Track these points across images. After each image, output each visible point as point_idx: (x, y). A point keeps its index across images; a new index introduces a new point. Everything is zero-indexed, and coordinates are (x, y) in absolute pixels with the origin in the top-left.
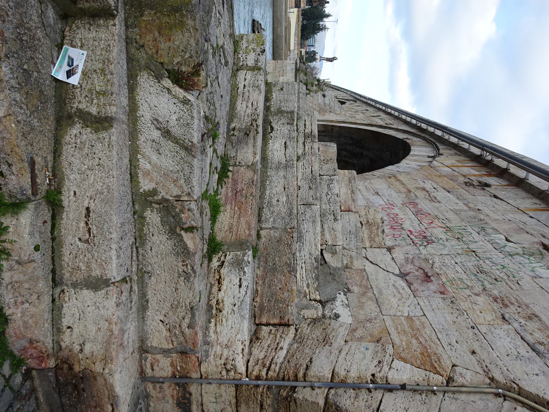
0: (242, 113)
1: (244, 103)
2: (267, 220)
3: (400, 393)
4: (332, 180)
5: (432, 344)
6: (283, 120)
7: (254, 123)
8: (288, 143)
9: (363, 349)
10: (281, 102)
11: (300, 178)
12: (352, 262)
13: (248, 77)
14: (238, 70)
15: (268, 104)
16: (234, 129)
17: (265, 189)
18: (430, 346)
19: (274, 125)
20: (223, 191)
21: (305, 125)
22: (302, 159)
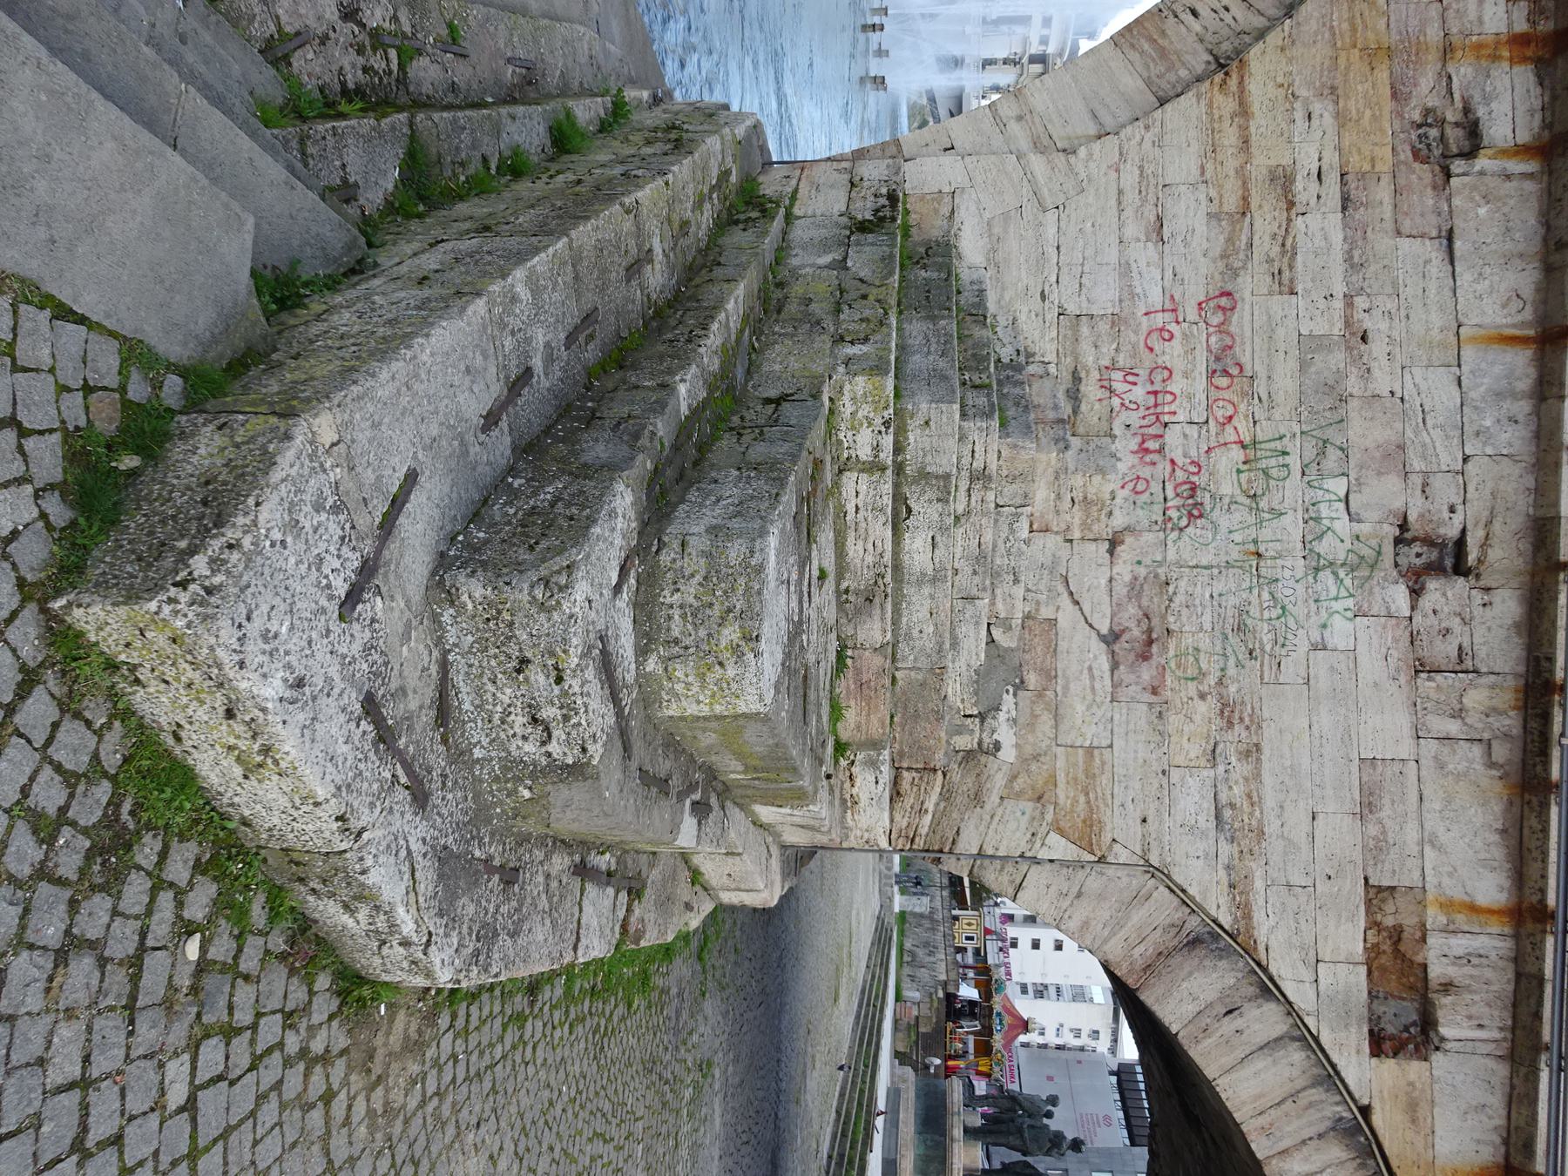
0: (857, 561)
1: (860, 543)
2: (904, 659)
3: (1048, 866)
4: (1018, 515)
6: (931, 494)
7: (880, 582)
8: (938, 538)
9: (1019, 814)
11: (957, 556)
13: (863, 488)
14: (841, 471)
16: (847, 591)
17: (900, 616)
20: (843, 683)
22: (963, 521)
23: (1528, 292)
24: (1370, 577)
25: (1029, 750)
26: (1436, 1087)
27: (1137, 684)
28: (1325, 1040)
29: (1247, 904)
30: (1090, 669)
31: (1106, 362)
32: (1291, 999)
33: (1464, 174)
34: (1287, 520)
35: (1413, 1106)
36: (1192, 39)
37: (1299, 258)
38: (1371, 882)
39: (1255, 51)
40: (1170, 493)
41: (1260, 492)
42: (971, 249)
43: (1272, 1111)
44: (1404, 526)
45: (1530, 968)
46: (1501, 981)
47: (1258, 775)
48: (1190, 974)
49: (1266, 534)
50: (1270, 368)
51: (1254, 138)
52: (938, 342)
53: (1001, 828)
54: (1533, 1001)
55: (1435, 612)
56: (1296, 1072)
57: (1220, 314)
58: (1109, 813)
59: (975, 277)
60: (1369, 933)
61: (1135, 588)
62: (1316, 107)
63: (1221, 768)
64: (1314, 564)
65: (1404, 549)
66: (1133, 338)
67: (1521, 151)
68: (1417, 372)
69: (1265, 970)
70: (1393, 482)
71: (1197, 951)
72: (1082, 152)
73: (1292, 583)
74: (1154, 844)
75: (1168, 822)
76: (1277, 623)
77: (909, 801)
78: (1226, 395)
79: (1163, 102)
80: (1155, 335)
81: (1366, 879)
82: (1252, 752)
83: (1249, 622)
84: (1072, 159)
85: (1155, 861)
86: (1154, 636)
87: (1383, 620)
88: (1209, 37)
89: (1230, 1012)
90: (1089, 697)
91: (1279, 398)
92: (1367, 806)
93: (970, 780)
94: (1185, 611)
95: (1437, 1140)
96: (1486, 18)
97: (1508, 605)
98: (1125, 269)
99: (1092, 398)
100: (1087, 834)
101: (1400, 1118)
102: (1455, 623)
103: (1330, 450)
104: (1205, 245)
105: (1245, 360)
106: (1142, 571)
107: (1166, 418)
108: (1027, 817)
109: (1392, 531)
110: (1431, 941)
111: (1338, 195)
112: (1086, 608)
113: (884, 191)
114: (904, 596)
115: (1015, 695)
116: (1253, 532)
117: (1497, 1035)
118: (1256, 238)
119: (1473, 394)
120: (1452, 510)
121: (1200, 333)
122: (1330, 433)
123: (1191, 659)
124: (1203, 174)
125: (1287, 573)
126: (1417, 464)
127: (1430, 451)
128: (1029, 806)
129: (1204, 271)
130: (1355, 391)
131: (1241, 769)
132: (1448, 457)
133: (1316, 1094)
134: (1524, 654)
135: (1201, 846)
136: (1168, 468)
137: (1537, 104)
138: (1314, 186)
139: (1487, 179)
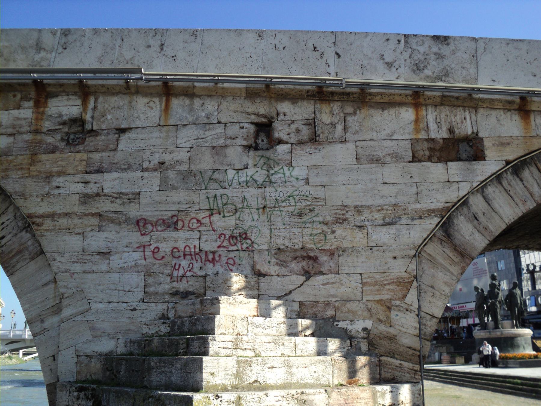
3: (421, 302)
5: (390, 277)
7: (296, 397)
8: (269, 365)
9: (398, 318)
10: (228, 374)
12: (295, 311)
15: (230, 388)
17: (307, 383)
18: (391, 279)
19: (252, 380)
21: (223, 348)
22: (257, 352)
23: (146, 100)
24: (274, 160)
25: (366, 314)
26: (493, 135)
27: (329, 262)
28: (482, 179)
29: (428, 211)
30: (323, 284)
31: (168, 279)
32: (467, 192)
33: (92, 124)
34: (247, 195)
35: (503, 144)
36: (14, 239)
37: (123, 191)
38: (411, 160)
39: (25, 211)
40: (234, 248)
41: (234, 207)
42: (106, 346)
43: (515, 200)
44: (248, 147)
45: (439, 100)
46: (445, 111)
47: (369, 207)
48: (462, 235)
49: (254, 204)
50: (174, 203)
51: (65, 211)
52: (165, 367)
53: (405, 326)
54: (452, 99)
55: (289, 134)
56: (497, 190)
57: (147, 226)
58: (393, 274)
59: (122, 345)
60: (433, 161)
61: (282, 264)
62: (55, 184)
63: (367, 223)
64: (268, 183)
65: (260, 146)
66: (157, 266)
67: (85, 103)
68: (179, 141)
69: (456, 204)
70: (230, 151)
71: (452, 233)
72: (62, 290)
73: (277, 193)
74: (405, 253)
75: (394, 246)
76: (297, 199)
77: (397, 374)
78: (186, 222)
79: (42, 252)
80: (156, 255)
81: (410, 162)
82: (358, 209)
83: (296, 212)
84: (66, 295)
85: (413, 252)
86: (305, 254)
87: (293, 155)
88: (14, 232)
89: (476, 218)
90: (337, 284)
91: (188, 199)
92: (377, 161)
93: (383, 342)
94: (292, 241)
95: (514, 135)
96: (25, 116)
97: (285, 107)
98: (122, 270)
99: (186, 285)
100: (405, 285)
101: (508, 149)
102: (293, 127)
103: (213, 177)
104: (114, 232)
105: (170, 214)
106: (273, 261)
107: (197, 250)
108: (398, 313)
109: (252, 153)
110: (433, 137)
111: (96, 175)
112: (293, 287)
113: (76, 394)
114: (298, 382)
115: (338, 321)
116: (253, 210)
117: (467, 113)
118: (112, 210)
119: (190, 119)
120: (242, 128)
121: (155, 234)
122: (206, 177)
123: (316, 237)
124: (79, 234)
125: (273, 195)
126: (221, 141)
127: (215, 136)
128: (393, 313)
129: (126, 233)
130: (187, 167)
131: (366, 214)
132: (220, 130)
133: (505, 183)
134: (305, 101)
135: (404, 232)
136: (222, 249)
137: (65, 97)
138: (91, 185)
139: (96, 115)
